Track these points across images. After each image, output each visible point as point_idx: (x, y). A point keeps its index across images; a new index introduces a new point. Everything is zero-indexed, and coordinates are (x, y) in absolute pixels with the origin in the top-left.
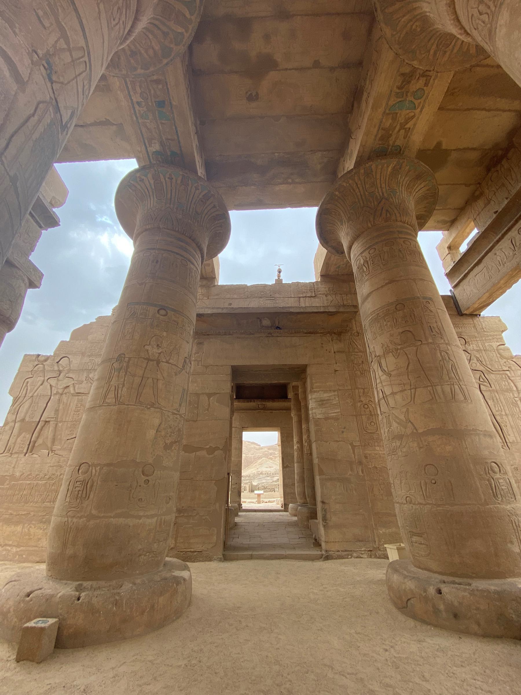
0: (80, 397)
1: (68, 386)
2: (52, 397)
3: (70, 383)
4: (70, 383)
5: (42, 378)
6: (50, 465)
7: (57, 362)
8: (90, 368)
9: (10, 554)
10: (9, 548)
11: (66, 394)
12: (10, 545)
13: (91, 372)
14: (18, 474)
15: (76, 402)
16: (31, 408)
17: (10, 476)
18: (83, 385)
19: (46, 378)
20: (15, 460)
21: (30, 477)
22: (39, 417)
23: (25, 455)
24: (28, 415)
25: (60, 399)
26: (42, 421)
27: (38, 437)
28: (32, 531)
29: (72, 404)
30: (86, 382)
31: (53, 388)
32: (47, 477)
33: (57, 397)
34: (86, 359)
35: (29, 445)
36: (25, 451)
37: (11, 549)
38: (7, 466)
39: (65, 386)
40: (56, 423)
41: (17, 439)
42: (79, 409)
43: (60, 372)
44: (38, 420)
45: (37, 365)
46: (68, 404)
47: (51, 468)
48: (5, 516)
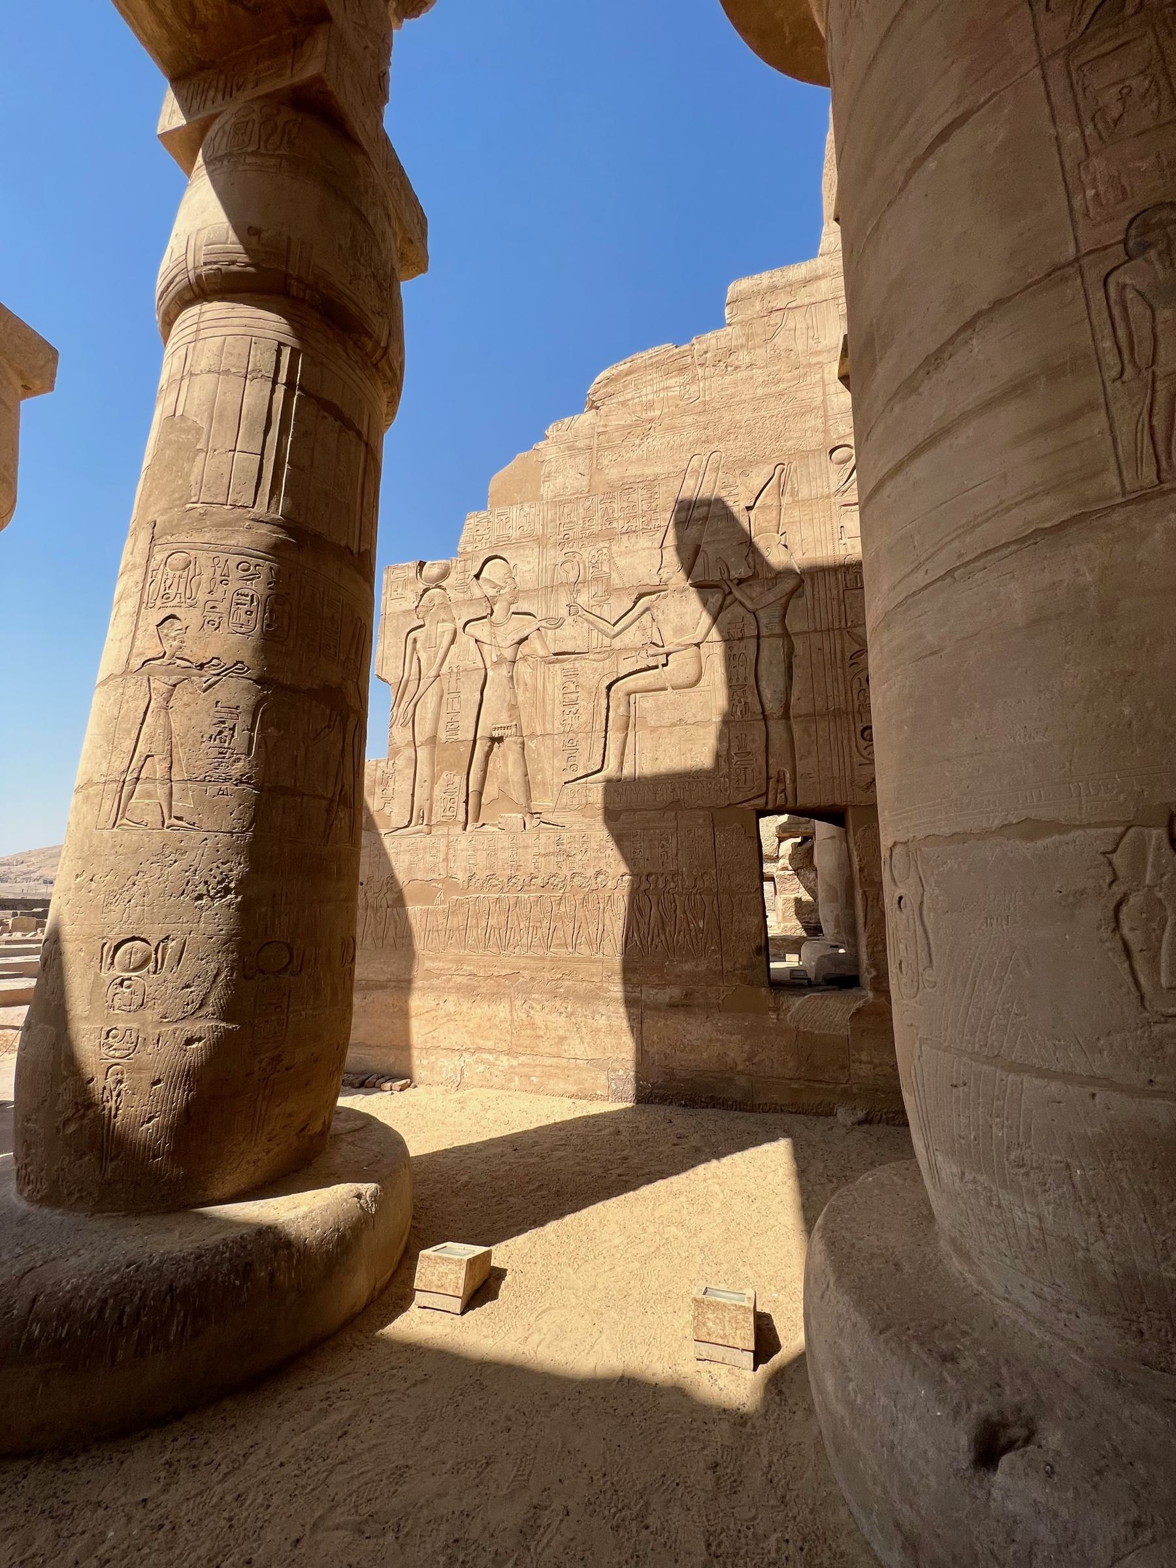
0: (567, 665)
1: (526, 638)
2: (490, 673)
3: (527, 626)
4: (527, 626)
5: (449, 626)
6: (536, 850)
7: (477, 576)
11: (524, 658)
14: (461, 877)
15: (559, 681)
16: (444, 707)
17: (443, 881)
18: (567, 630)
20: (444, 841)
24: (442, 725)
25: (512, 677)
26: (482, 738)
28: (538, 1017)
29: (549, 687)
30: (570, 620)
31: (486, 648)
34: (555, 555)
35: (467, 802)
38: (429, 858)
39: (517, 638)
40: (520, 740)
41: (432, 789)
42: (574, 696)
43: (491, 601)
45: (426, 591)
46: (540, 687)
48: (459, 979)
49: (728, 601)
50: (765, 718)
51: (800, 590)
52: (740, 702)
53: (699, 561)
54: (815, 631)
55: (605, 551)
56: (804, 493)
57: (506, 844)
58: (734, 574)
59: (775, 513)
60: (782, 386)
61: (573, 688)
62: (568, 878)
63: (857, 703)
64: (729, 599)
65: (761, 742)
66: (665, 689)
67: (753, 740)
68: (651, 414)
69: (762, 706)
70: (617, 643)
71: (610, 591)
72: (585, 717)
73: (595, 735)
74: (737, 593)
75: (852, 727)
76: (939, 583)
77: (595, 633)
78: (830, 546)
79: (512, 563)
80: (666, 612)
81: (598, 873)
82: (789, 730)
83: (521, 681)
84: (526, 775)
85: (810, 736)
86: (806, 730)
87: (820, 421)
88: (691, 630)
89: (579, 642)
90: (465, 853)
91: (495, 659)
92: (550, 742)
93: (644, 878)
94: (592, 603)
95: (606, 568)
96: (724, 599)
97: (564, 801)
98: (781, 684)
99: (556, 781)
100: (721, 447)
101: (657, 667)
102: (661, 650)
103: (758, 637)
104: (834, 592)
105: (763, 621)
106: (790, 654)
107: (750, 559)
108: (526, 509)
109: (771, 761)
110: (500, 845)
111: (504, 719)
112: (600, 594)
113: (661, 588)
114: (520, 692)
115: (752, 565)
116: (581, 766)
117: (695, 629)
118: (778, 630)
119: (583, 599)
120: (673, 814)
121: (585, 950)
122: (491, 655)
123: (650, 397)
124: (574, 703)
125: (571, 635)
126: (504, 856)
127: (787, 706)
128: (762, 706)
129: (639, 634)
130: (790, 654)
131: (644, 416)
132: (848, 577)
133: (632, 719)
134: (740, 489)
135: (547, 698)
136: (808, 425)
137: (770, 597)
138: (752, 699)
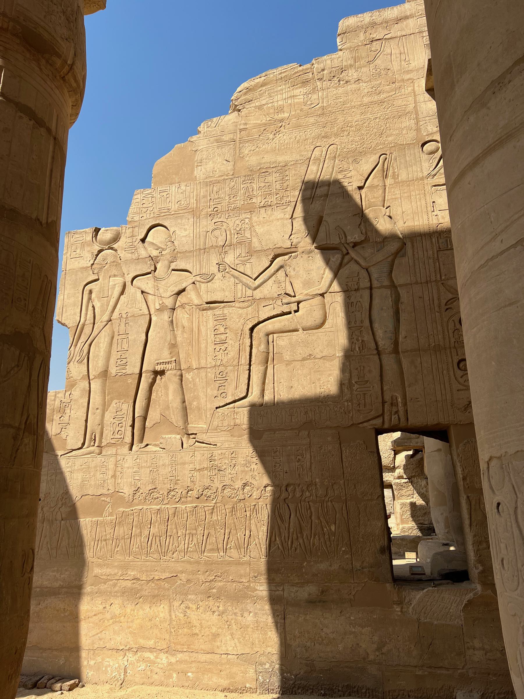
0: (218, 312)
1: (184, 290)
2: (154, 318)
5: (119, 280)
6: (192, 466)
7: (143, 240)
9: (156, 670)
10: (152, 656)
11: (182, 306)
12: (151, 650)
13: (226, 252)
14: (127, 491)
15: (211, 323)
16: (114, 346)
17: (111, 496)
18: (217, 283)
19: (129, 278)
20: (113, 459)
21: (156, 495)
23: (131, 449)
24: (112, 361)
25: (172, 322)
26: (146, 371)
28: (193, 616)
29: (203, 329)
30: (219, 275)
31: (150, 298)
32: (194, 493)
34: (207, 224)
35: (133, 426)
36: (128, 439)
37: (156, 657)
38: (99, 476)
39: (176, 290)
40: (179, 373)
42: (223, 337)
43: (155, 260)
44: (137, 371)
45: (100, 251)
46: (195, 330)
47: (196, 474)
48: (124, 584)
49: (346, 260)
50: (379, 354)
53: (322, 229)
54: (417, 283)
55: (247, 221)
56: (403, 176)
57: (167, 462)
58: (351, 239)
59: (381, 192)
60: (382, 96)
61: (222, 330)
62: (220, 490)
63: (453, 340)
64: (347, 258)
65: (376, 373)
66: (297, 330)
67: (370, 371)
68: (281, 116)
69: (376, 343)
70: (258, 294)
71: (251, 252)
72: (232, 353)
73: (241, 368)
74: (353, 254)
75: (450, 360)
76: (512, 250)
77: (239, 286)
78: (425, 217)
79: (172, 230)
80: (297, 269)
81: (245, 485)
83: (180, 324)
84: (184, 402)
87: (413, 122)
88: (317, 283)
89: (227, 293)
90: (130, 470)
91: (158, 307)
92: (204, 374)
93: (283, 488)
94: (237, 262)
95: (248, 235)
96: (343, 259)
97: (215, 423)
99: (209, 406)
100: (337, 141)
101: (290, 313)
102: (293, 299)
103: (371, 288)
104: (430, 252)
105: (374, 276)
106: (397, 301)
107: (362, 227)
108: (183, 187)
109: (385, 388)
110: (161, 463)
111: (166, 356)
112: (243, 255)
113: (292, 250)
114: (179, 333)
115: (364, 232)
116: (229, 394)
117: (320, 282)
118: (386, 283)
119: (230, 259)
120: (307, 433)
121: (234, 553)
122: (155, 304)
123: (280, 103)
124: (223, 342)
125: (220, 288)
126: (164, 471)
127: (396, 343)
128: (376, 343)
129: (275, 286)
130: (397, 301)
131: (276, 117)
132: (440, 241)
133: (271, 355)
134: (353, 173)
135: (201, 339)
136: (404, 125)
137: (379, 257)
138: (367, 337)
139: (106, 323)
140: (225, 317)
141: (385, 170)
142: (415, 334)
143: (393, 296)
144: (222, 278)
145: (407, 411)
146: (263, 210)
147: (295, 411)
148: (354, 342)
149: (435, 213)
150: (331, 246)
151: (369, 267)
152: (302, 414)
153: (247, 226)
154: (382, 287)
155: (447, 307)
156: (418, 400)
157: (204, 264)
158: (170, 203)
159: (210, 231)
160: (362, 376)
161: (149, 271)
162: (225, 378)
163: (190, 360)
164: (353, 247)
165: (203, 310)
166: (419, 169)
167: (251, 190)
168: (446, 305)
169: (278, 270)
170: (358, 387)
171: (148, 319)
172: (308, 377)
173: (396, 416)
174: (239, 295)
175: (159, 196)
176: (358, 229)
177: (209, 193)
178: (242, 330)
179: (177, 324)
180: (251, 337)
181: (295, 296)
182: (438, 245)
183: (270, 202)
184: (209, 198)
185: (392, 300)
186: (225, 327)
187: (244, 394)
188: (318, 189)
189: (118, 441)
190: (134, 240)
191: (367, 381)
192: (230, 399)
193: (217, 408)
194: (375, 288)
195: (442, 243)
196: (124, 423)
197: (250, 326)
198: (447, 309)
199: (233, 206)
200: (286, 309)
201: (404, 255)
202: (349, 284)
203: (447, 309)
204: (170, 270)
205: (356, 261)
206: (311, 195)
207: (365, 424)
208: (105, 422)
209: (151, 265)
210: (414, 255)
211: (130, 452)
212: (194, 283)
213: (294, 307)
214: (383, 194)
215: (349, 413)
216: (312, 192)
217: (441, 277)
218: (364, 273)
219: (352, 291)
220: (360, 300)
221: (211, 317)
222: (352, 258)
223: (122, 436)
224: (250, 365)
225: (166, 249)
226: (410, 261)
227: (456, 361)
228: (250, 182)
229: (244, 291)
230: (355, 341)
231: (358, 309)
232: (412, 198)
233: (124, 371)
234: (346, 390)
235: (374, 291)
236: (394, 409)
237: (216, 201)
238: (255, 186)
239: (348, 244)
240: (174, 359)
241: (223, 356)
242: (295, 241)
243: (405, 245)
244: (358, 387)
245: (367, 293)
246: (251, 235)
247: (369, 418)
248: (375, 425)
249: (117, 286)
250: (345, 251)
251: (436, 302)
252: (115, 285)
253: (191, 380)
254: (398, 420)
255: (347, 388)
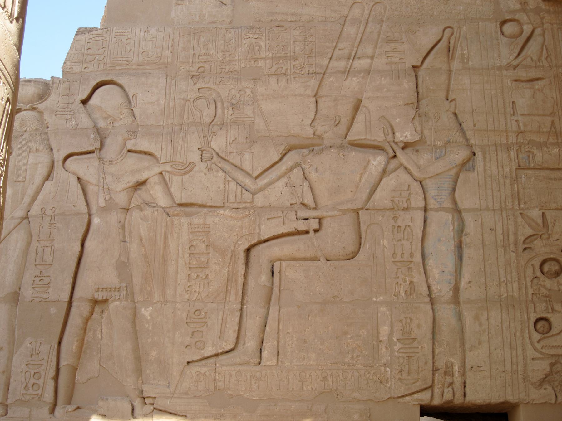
0: (197, 221)
1: (144, 183)
2: (96, 221)
7: (84, 102)
8: (207, 120)
13: (214, 134)
19: (59, 156)
22: (69, 287)
23: (52, 411)
24: (28, 277)
27: (80, 353)
33: (114, 217)
35: (56, 378)
36: (49, 396)
39: (133, 180)
41: (10, 359)
50: (432, 301)
51: (471, 163)
52: (405, 281)
54: (487, 209)
55: (248, 92)
63: (530, 292)
64: (394, 164)
67: (419, 326)
70: (259, 200)
77: (233, 185)
82: (460, 317)
85: (481, 325)
86: (476, 318)
91: (102, 203)
96: (388, 163)
98: (450, 262)
101: (307, 232)
103: (426, 210)
104: (507, 170)
105: (432, 192)
106: (461, 231)
108: (153, 31)
111: (110, 277)
115: (418, 129)
118: (448, 204)
125: (204, 184)
127: (456, 290)
128: (429, 288)
130: (461, 231)
132: (520, 156)
133: (276, 290)
137: (439, 167)
138: (418, 278)
139: (19, 220)
140: (207, 230)
141: (451, 49)
142: (483, 280)
143: (456, 223)
144: (205, 171)
145: (465, 383)
146: (273, 80)
147: (308, 375)
148: (399, 283)
149: (515, 118)
150: (372, 143)
151: (425, 179)
152: (318, 380)
153: (247, 99)
154: (441, 209)
155: (526, 246)
156: (481, 369)
157: (180, 147)
158: (131, 53)
159: (192, 100)
160: (408, 330)
161: (92, 148)
162: (204, 320)
163: (149, 289)
164: (403, 148)
165: (175, 215)
166: (496, 55)
167: (257, 48)
168: (524, 242)
169: (291, 169)
170: (401, 346)
171: (87, 220)
172: (330, 328)
173: (450, 389)
174: (232, 198)
175: (114, 40)
176: (410, 125)
177: (192, 45)
178: (233, 251)
179: (130, 232)
180: (247, 263)
181: (315, 209)
182: (517, 161)
183: (284, 69)
184: (192, 52)
185: (453, 229)
186: (206, 244)
187: (233, 346)
188: (356, 60)
189: (33, 398)
190: (71, 101)
191: (414, 339)
192: (209, 351)
193: (188, 363)
194: (431, 210)
195: (523, 158)
196: (43, 374)
197: (246, 246)
198: (525, 249)
199: (228, 67)
200: (302, 226)
201: (473, 169)
202: (396, 200)
203: (525, 249)
204: (125, 151)
205: (406, 168)
206: (346, 68)
207: (408, 399)
208: (13, 368)
209: (95, 139)
210: (485, 170)
211: (51, 416)
212: (161, 173)
213: (314, 224)
214: (447, 81)
215: (387, 382)
216: (347, 64)
217: (519, 204)
218: (416, 186)
219: (398, 210)
220: (410, 224)
221: (185, 226)
222: (401, 165)
223: (39, 392)
224: (242, 304)
225: (121, 119)
226: (480, 177)
227: (533, 319)
228: (256, 37)
229: (239, 193)
230: (401, 282)
231: (406, 237)
232: (486, 92)
233: (45, 296)
234: (384, 350)
235: (430, 214)
236: (448, 379)
237: (203, 57)
238: (262, 44)
239: (396, 143)
240: (124, 284)
241: (202, 287)
242: (320, 129)
243: (474, 155)
244: (401, 346)
245: (420, 215)
246: (254, 113)
247: (413, 391)
248: (422, 400)
249: (39, 166)
250: (391, 154)
251: (512, 238)
252: (37, 164)
253: (149, 318)
254: (452, 395)
255: (386, 348)
